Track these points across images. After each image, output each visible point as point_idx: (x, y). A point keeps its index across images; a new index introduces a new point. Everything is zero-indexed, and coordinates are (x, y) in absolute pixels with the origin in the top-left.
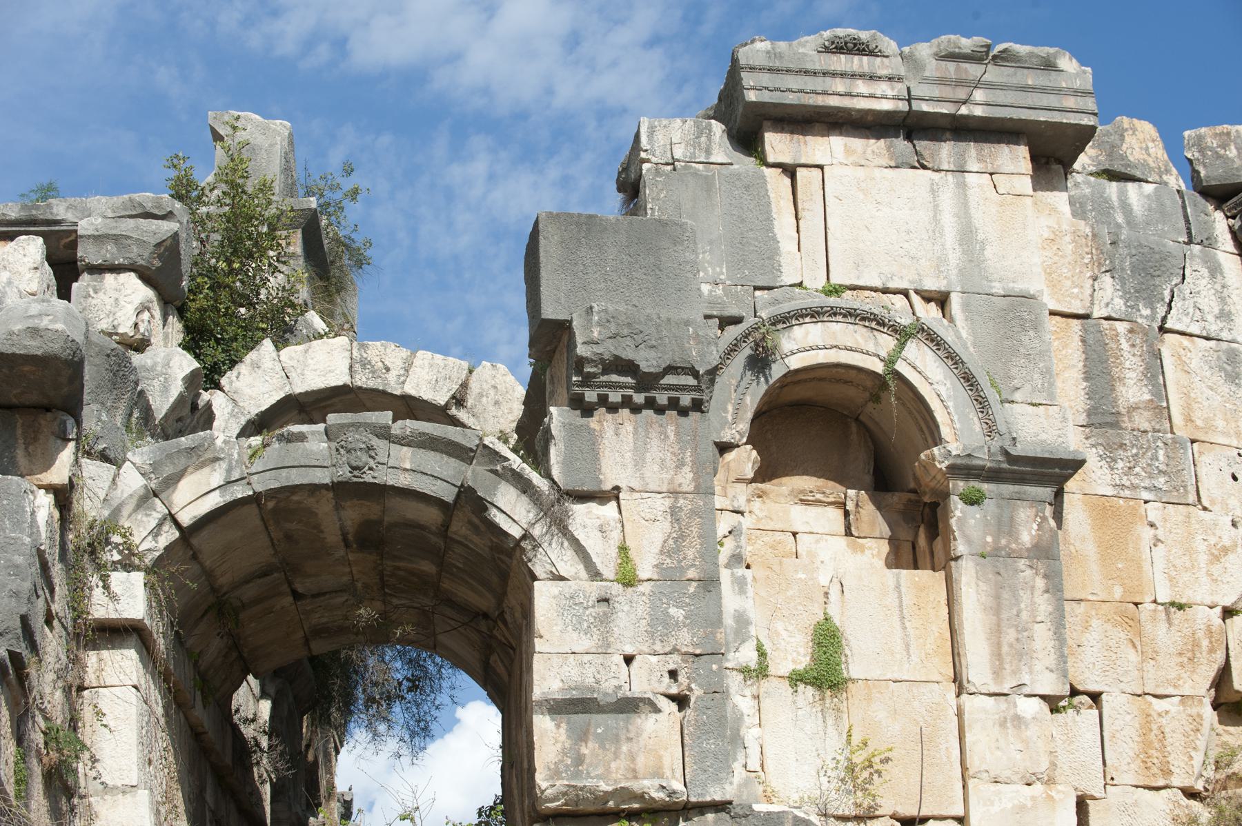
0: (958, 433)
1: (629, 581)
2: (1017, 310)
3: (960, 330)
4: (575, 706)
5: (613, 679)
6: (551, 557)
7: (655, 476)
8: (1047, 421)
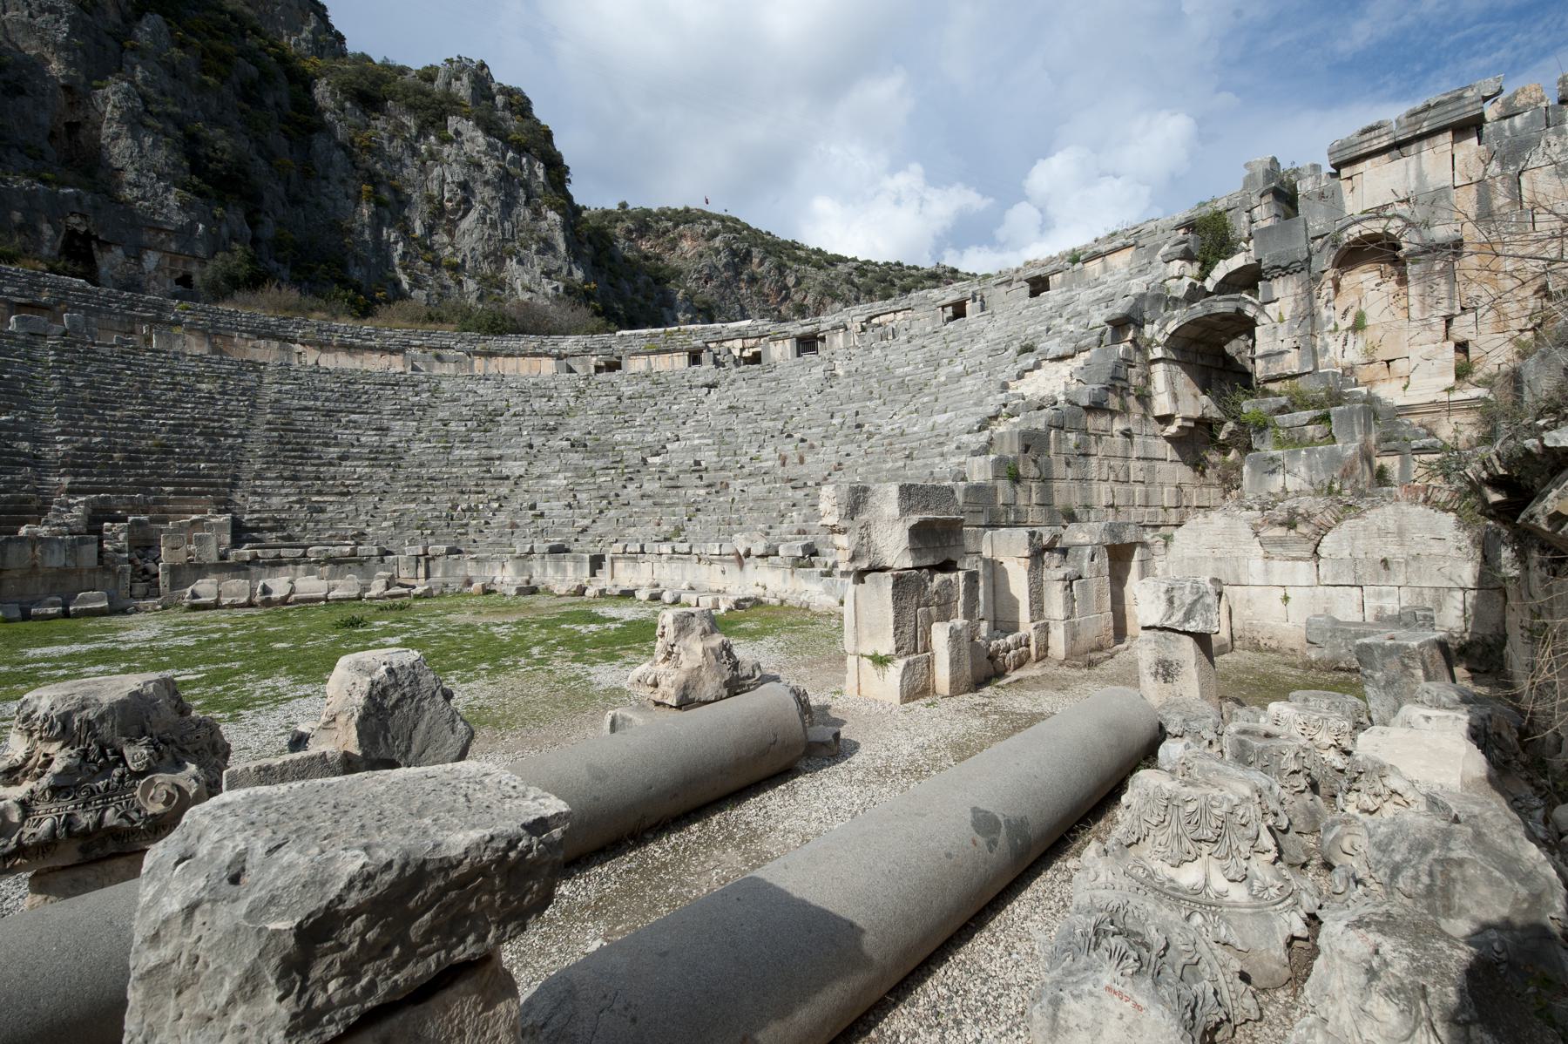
1: (1282, 321)
5: (1279, 346)
6: (1261, 319)
7: (1290, 291)
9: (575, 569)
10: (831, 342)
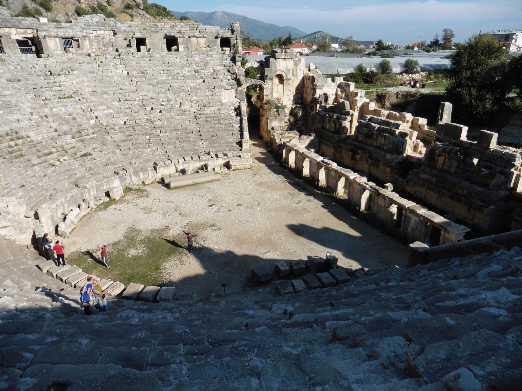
0: (285, 77)
2: (289, 70)
3: (286, 72)
4: (266, 95)
5: (268, 94)
6: (265, 87)
9: (143, 174)
10: (83, 44)
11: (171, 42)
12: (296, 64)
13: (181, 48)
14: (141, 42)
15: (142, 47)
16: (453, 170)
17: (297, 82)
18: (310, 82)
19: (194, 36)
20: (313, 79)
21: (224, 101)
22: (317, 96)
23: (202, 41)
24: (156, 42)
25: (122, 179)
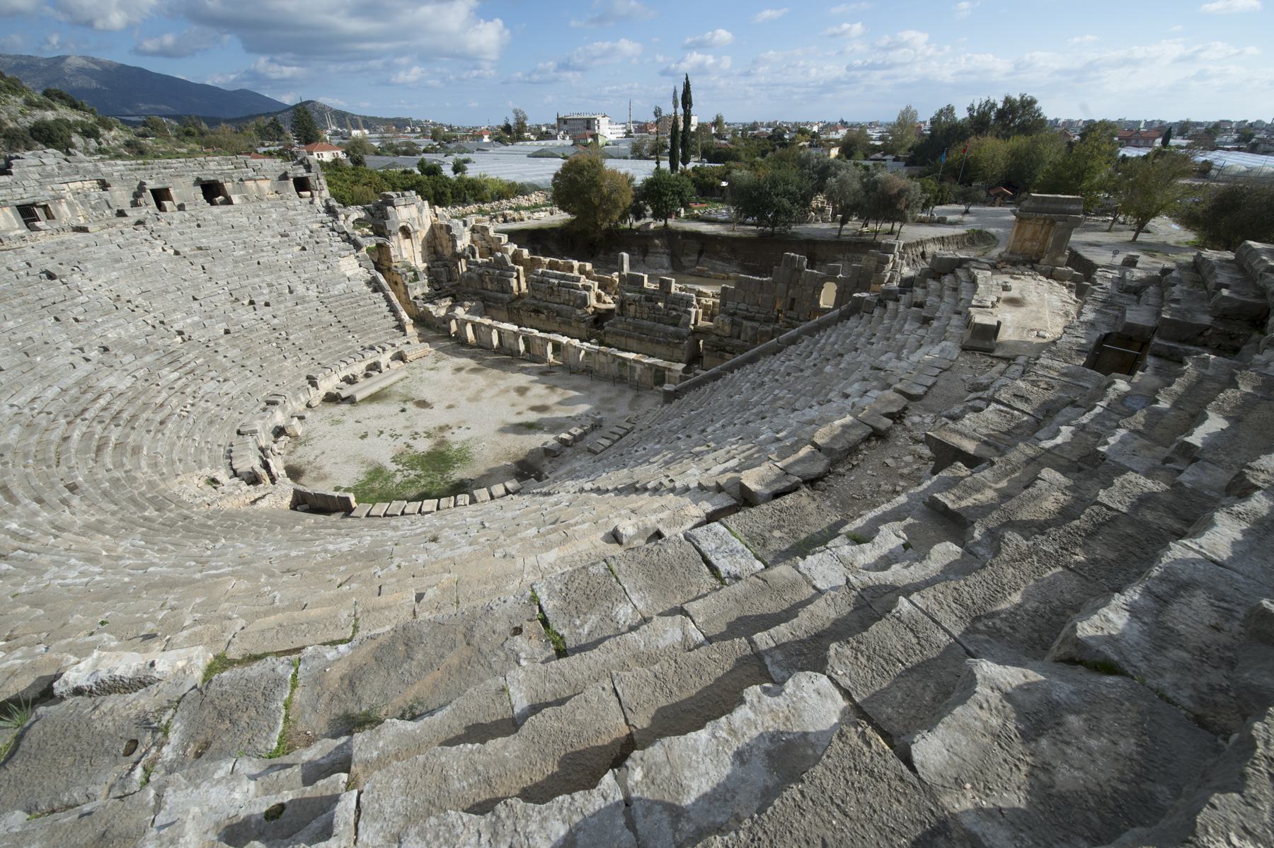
8: (417, 227)
10: (58, 211)
11: (212, 191)
12: (420, 211)
13: (236, 199)
14: (160, 196)
15: (167, 204)
16: (645, 316)
17: (423, 233)
18: (444, 232)
19: (250, 179)
20: (449, 228)
21: (349, 274)
22: (459, 249)
23: (265, 185)
24: (184, 190)
25: (284, 410)
